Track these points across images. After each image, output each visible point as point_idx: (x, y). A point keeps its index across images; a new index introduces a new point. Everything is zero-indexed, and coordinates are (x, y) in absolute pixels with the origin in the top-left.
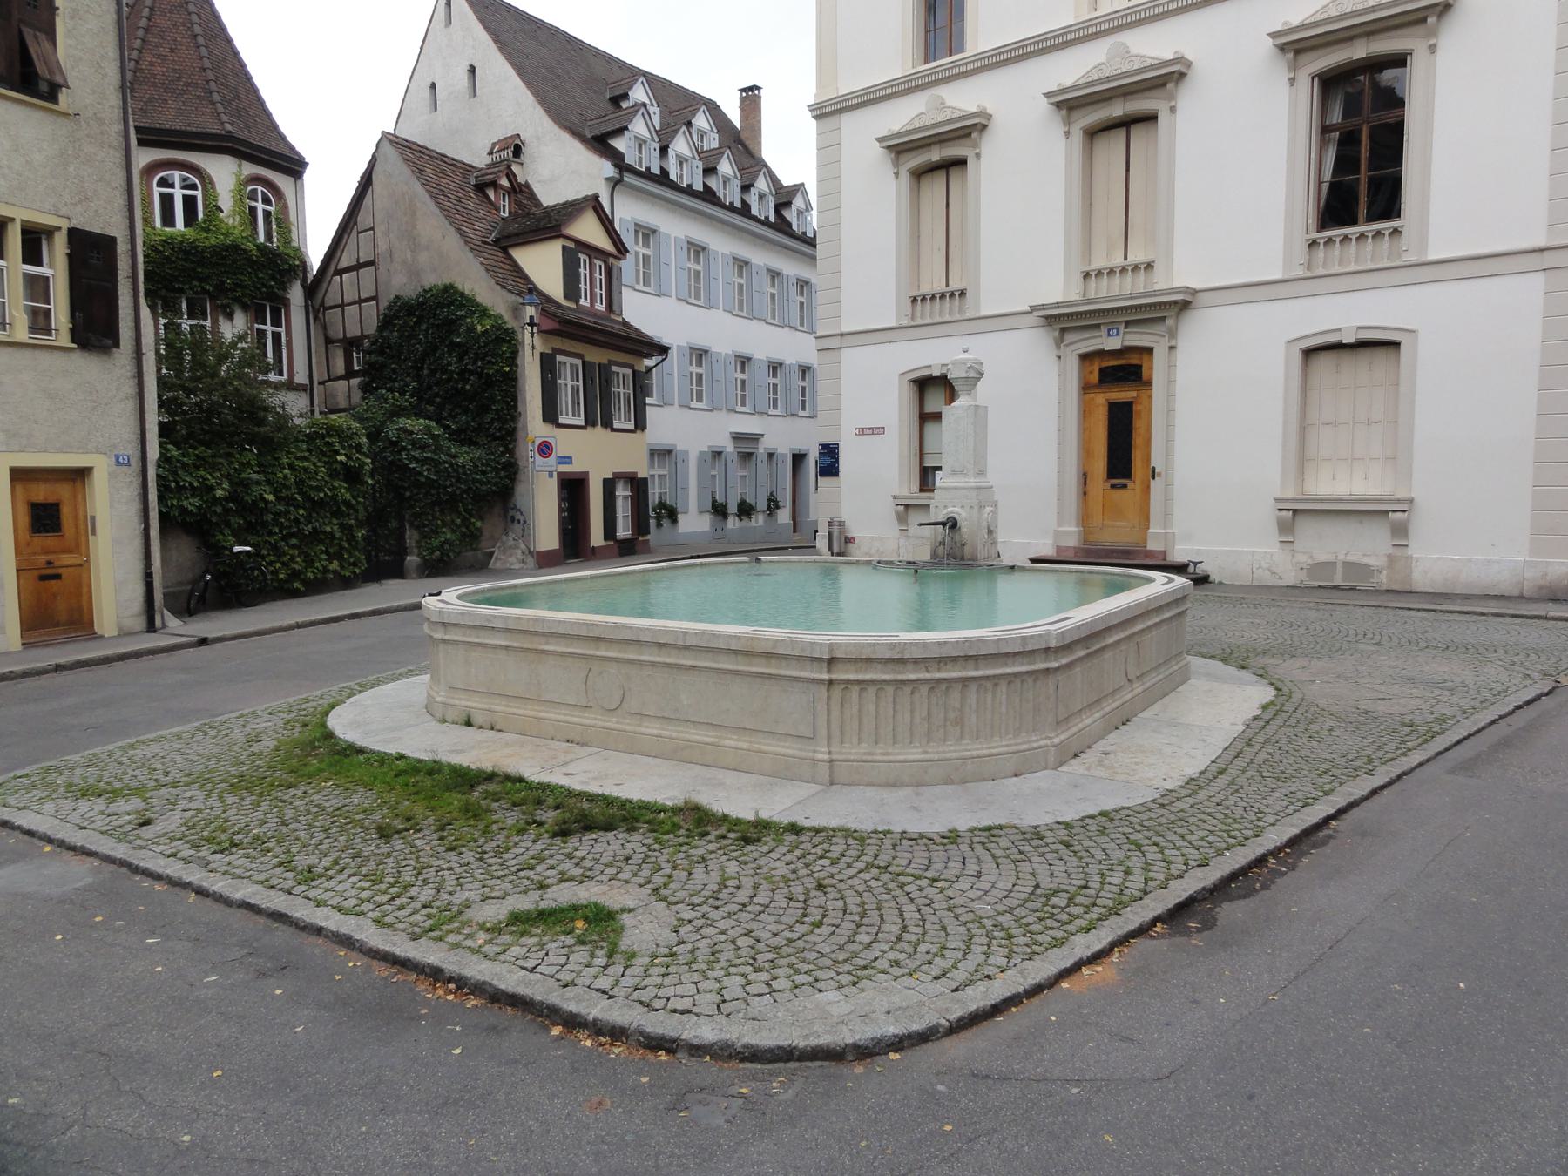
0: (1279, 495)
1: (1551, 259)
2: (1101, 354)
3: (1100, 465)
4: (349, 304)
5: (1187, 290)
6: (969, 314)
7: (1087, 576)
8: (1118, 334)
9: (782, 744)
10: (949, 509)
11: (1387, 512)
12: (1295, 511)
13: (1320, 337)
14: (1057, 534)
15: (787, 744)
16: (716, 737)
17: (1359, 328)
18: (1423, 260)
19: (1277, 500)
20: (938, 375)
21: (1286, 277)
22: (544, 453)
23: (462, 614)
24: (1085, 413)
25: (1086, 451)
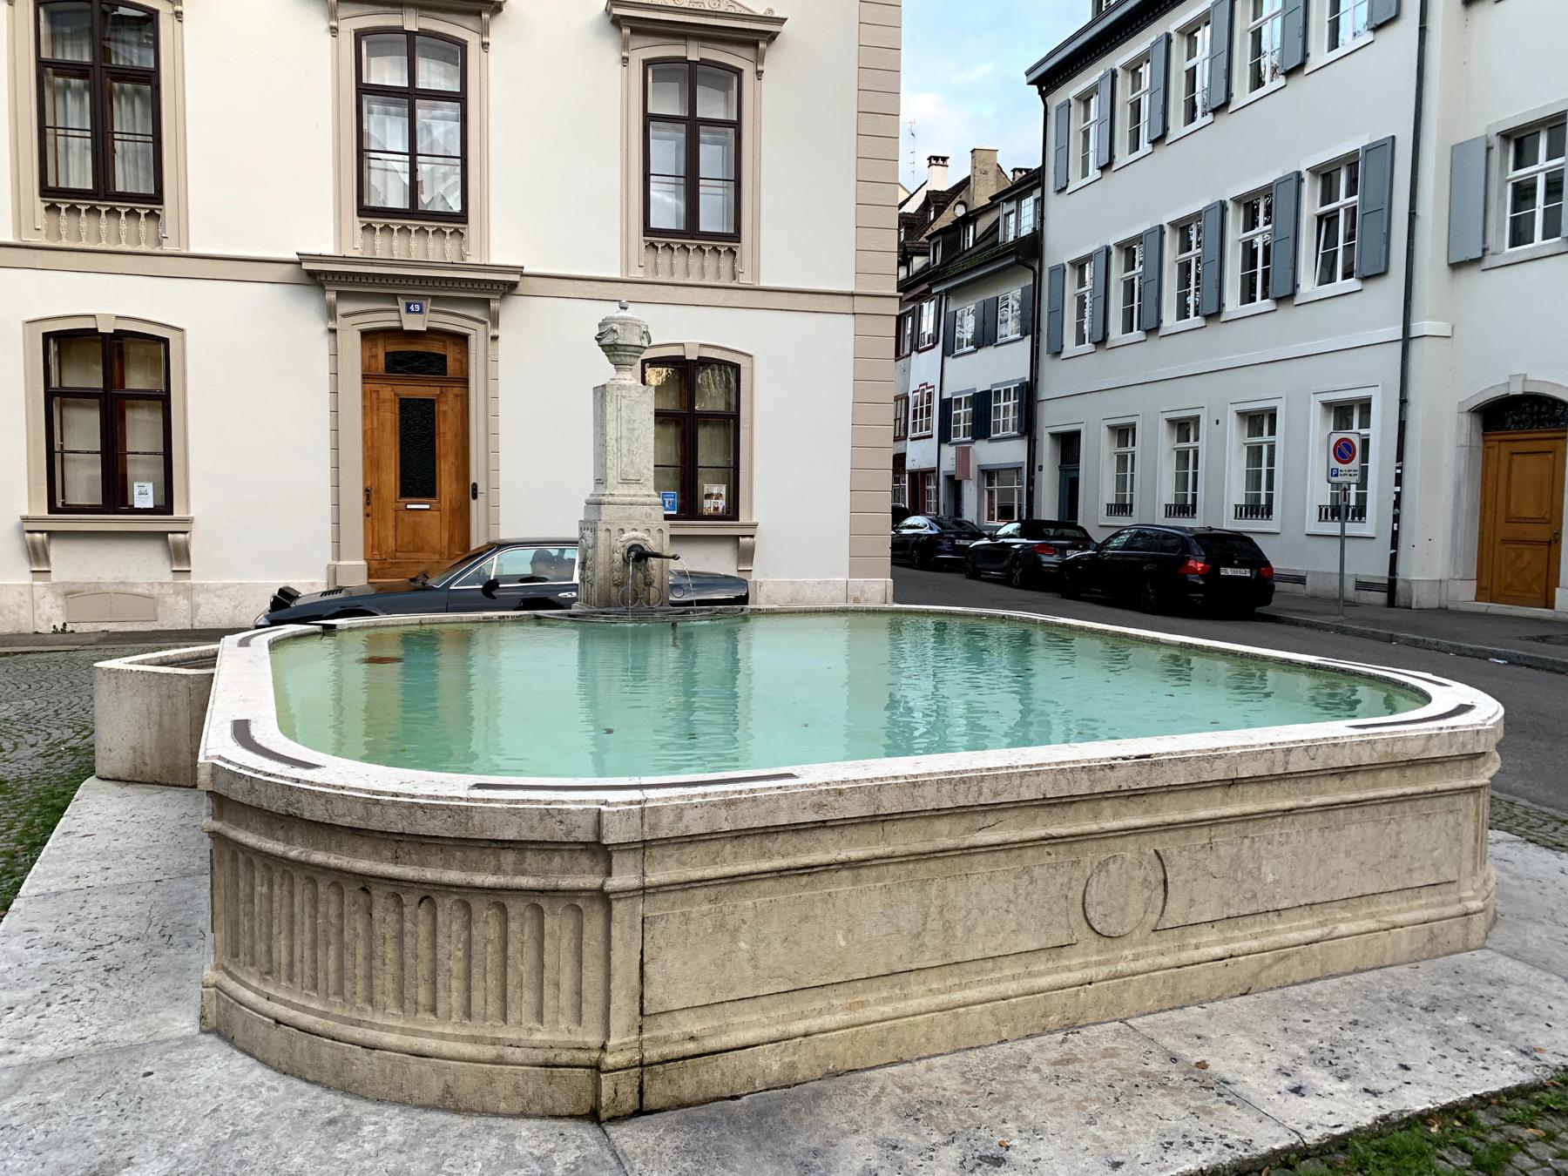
0: (26, 513)
1: (862, 305)
2: (398, 333)
3: (390, 478)
4: (692, 106)
5: (518, 270)
6: (168, 248)
7: (469, 626)
8: (421, 312)
9: (1416, 903)
10: (629, 534)
11: (737, 537)
12: (50, 533)
13: (59, 322)
14: (333, 572)
15: (1422, 902)
16: (1322, 924)
17: (702, 345)
18: (756, 285)
19: (25, 519)
20: (695, 358)
21: (625, 278)
22: (1344, 456)
23: (729, 804)
24: (370, 406)
25: (372, 463)
